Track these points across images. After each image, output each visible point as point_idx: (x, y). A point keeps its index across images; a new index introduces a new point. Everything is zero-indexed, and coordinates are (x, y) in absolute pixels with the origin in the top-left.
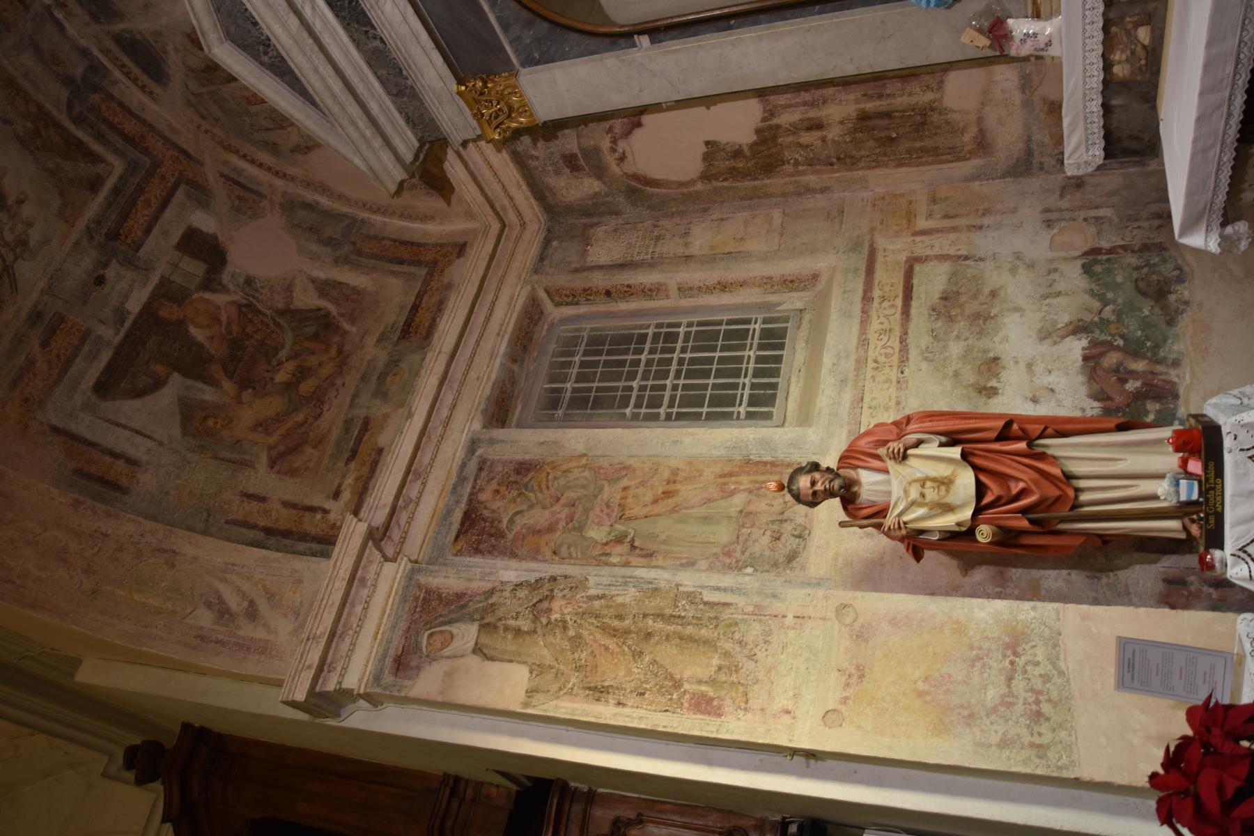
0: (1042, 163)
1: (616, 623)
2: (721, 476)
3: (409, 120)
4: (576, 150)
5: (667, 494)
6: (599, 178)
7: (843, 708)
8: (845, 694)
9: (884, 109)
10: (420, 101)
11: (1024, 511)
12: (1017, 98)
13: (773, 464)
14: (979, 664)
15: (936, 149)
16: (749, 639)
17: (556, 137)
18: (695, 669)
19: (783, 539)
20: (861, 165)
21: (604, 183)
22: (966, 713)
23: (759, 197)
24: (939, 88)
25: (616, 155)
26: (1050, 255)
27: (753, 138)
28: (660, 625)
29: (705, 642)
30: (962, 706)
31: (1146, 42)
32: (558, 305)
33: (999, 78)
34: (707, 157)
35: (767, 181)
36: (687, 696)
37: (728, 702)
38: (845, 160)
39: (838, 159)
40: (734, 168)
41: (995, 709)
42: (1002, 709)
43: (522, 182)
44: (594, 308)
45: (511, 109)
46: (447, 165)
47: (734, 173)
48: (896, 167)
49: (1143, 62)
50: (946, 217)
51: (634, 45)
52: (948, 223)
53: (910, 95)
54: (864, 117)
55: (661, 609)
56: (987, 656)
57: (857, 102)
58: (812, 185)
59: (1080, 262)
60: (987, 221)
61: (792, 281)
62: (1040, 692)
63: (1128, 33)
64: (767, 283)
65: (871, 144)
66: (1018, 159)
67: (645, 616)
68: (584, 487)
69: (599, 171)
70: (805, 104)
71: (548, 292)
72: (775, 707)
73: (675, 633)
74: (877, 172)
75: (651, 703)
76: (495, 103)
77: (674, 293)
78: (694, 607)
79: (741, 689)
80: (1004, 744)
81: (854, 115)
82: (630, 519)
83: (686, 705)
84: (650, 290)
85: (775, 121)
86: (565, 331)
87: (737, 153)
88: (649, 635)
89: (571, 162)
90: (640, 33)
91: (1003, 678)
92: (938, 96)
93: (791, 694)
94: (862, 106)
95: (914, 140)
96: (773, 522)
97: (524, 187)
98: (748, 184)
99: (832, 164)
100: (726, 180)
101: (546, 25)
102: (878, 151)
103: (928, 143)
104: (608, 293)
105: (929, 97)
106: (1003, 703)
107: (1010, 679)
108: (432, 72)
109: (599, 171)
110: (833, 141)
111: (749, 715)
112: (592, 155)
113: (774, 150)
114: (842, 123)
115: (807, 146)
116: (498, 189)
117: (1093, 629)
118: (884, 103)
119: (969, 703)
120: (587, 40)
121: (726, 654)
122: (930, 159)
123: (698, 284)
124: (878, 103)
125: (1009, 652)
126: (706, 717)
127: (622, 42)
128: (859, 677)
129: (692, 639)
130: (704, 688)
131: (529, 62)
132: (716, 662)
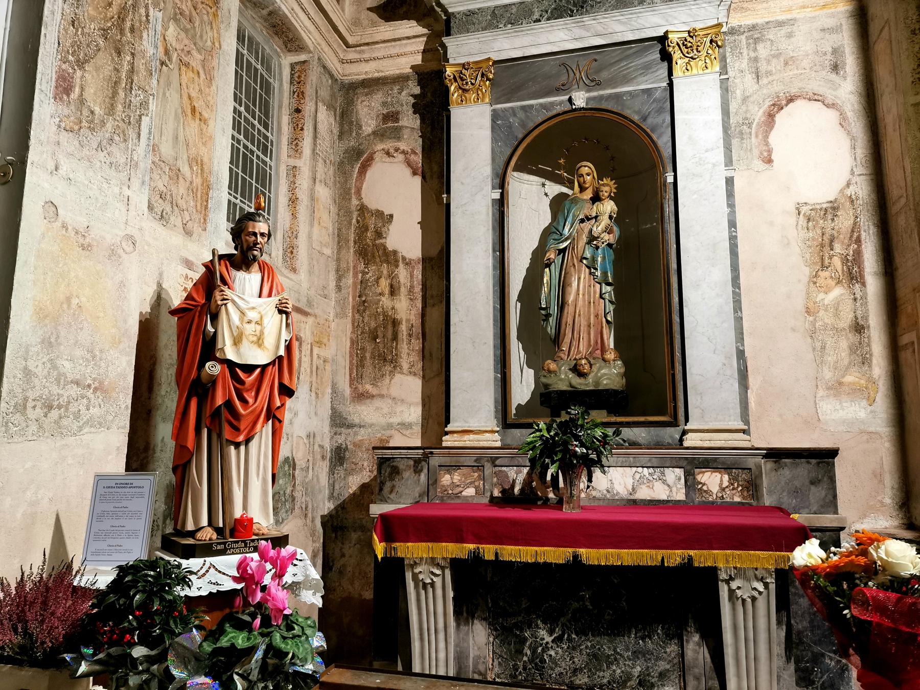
0: (340, 434)
1: (128, 24)
2: (202, 161)
3: (471, 13)
4: (401, 123)
5: (193, 110)
6: (374, 133)
7: (58, 224)
8: (70, 228)
9: (400, 336)
10: (484, 29)
11: (229, 404)
12: (395, 420)
13: (206, 207)
14: (89, 356)
15: (363, 367)
16: (114, 149)
17: (415, 113)
18: (92, 84)
19: (160, 201)
20: (357, 316)
21: (369, 135)
22: (52, 340)
23: (339, 243)
24: (410, 373)
25: (392, 151)
26: (295, 436)
27: (390, 247)
28: (126, 67)
29: (112, 105)
30: (58, 337)
31: (463, 493)
32: (292, 66)
33: (412, 409)
34: (379, 214)
35: (352, 250)
36: (71, 71)
37: (66, 111)
38: (362, 306)
39: (364, 302)
40: (367, 230)
41: (55, 367)
42: (55, 373)
43: (381, 74)
44: (286, 94)
45: (465, 91)
46: (413, 23)
47: (362, 229)
48: (352, 339)
49: (450, 492)
50: (317, 368)
51: (493, 188)
52: (314, 369)
53: (408, 354)
54: (395, 323)
55: (137, 73)
56: (95, 364)
57: (408, 321)
58: (344, 280)
59: (290, 456)
60: (313, 394)
61: (292, 253)
62: (67, 409)
63: (471, 483)
64: (293, 234)
65: (373, 325)
66: (346, 419)
67: (133, 54)
68: (201, 37)
69: (379, 134)
70: (412, 287)
71: (305, 62)
72: (60, 156)
73: (120, 78)
74: (349, 327)
75: (66, 30)
76: (473, 81)
77: (292, 162)
78: (138, 104)
79: (76, 128)
80: (27, 372)
81: (398, 317)
82: (180, 69)
83: (64, 66)
84: (297, 145)
85: (401, 265)
86: (274, 63)
87: (379, 234)
88: (119, 53)
89: (391, 117)
90: (502, 194)
91: (78, 377)
92: (405, 371)
93: (71, 176)
94: (404, 323)
95: (372, 353)
96: (171, 195)
97: (376, 75)
98: (352, 237)
99: (359, 296)
100: (358, 222)
101: (520, 136)
102: (367, 328)
103: (368, 362)
104: (298, 111)
105: (405, 366)
106: (59, 375)
107: (77, 383)
108: (506, 46)
109: (379, 134)
110: (379, 300)
111: (54, 128)
112: (396, 134)
113: (378, 260)
114: (393, 308)
115: (378, 283)
116: (379, 54)
117: (110, 457)
118: (404, 337)
119: (60, 344)
120: (504, 158)
121: (103, 123)
122: (354, 361)
123: (298, 182)
124: (405, 333)
125: (97, 384)
126: (54, 84)
127: (498, 181)
128: (82, 245)
129: (115, 94)
130: (77, 90)
131: (495, 116)
132: (97, 110)
